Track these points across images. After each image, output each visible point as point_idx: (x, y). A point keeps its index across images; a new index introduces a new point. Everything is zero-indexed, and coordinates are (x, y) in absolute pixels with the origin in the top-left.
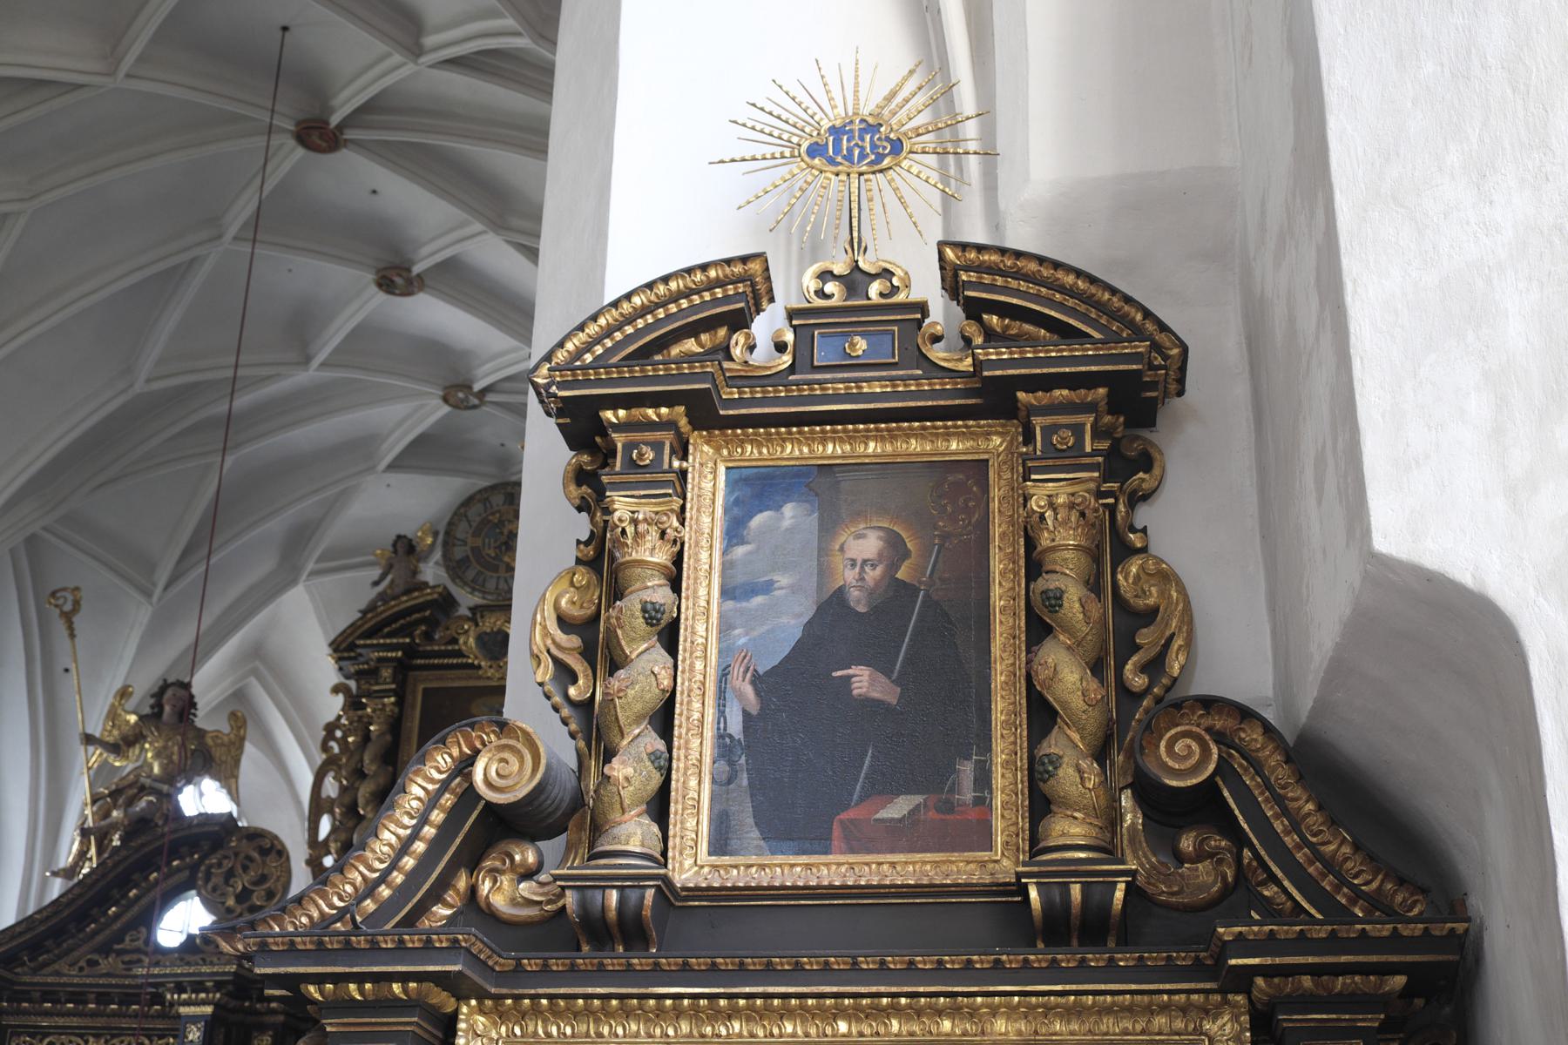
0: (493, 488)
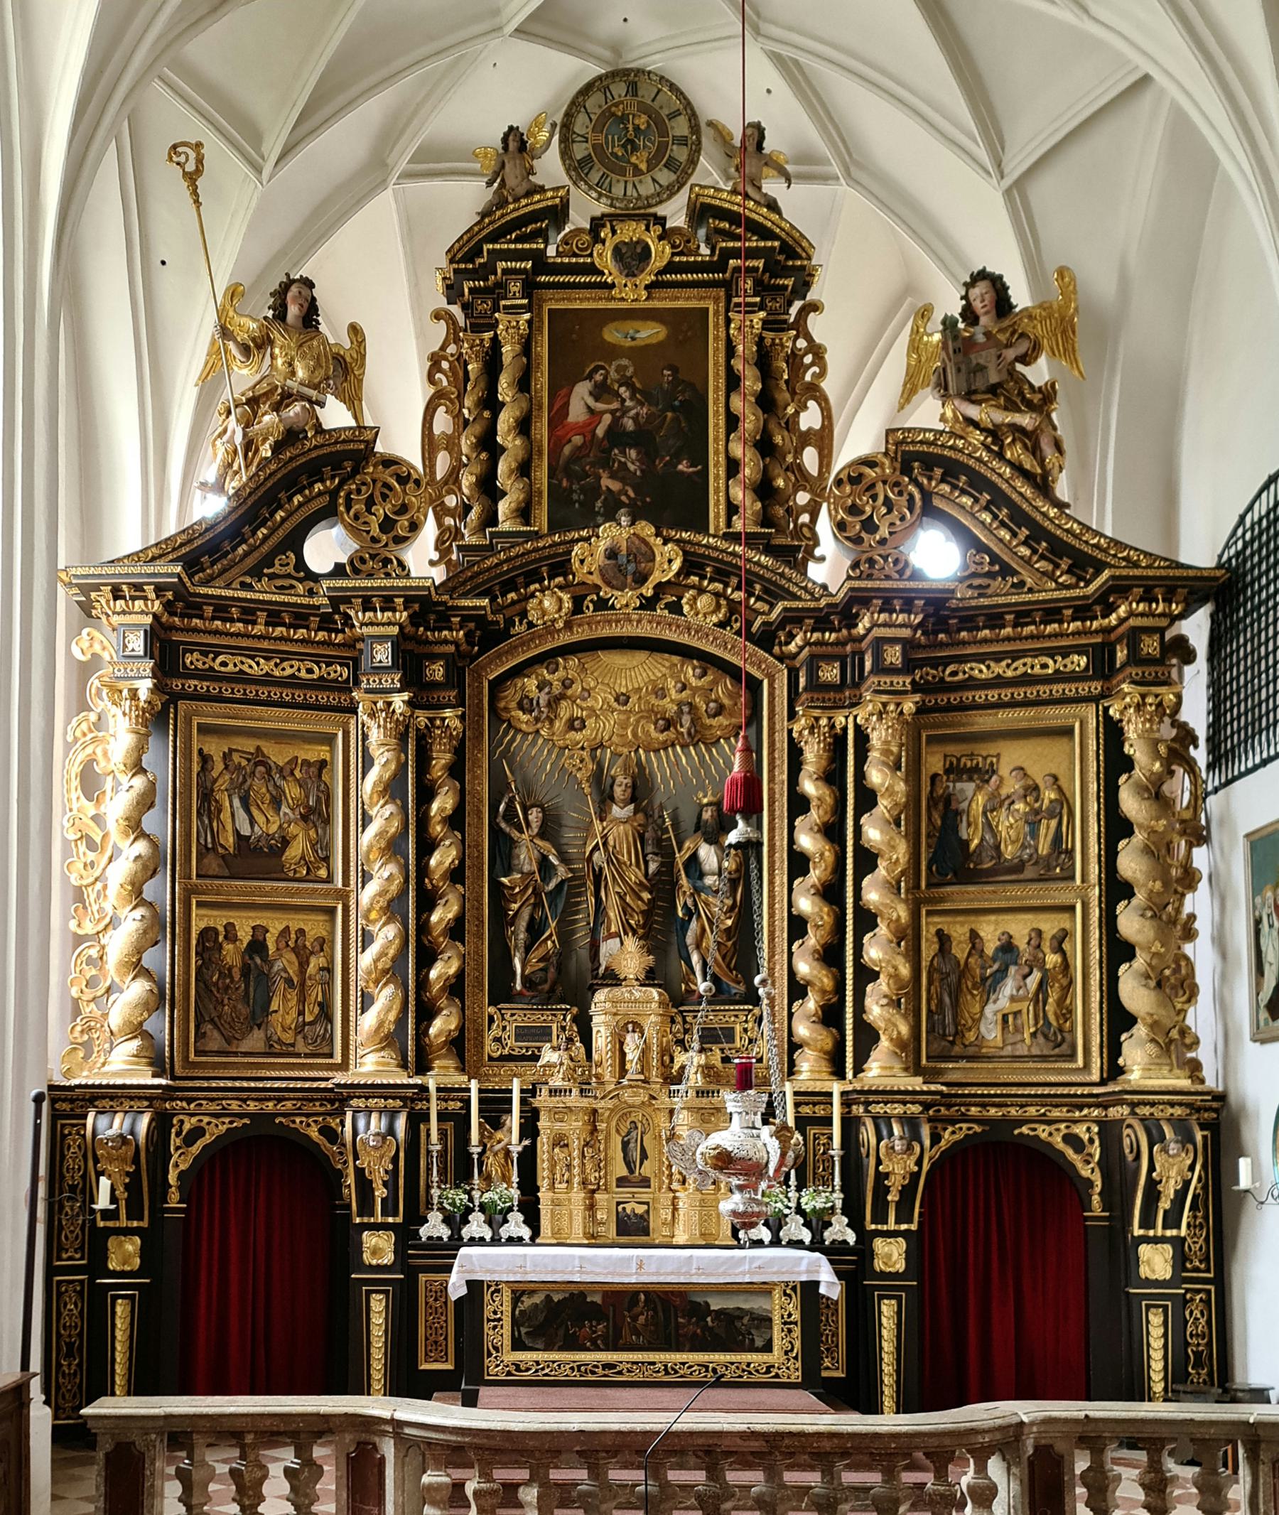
0: (614, 75)
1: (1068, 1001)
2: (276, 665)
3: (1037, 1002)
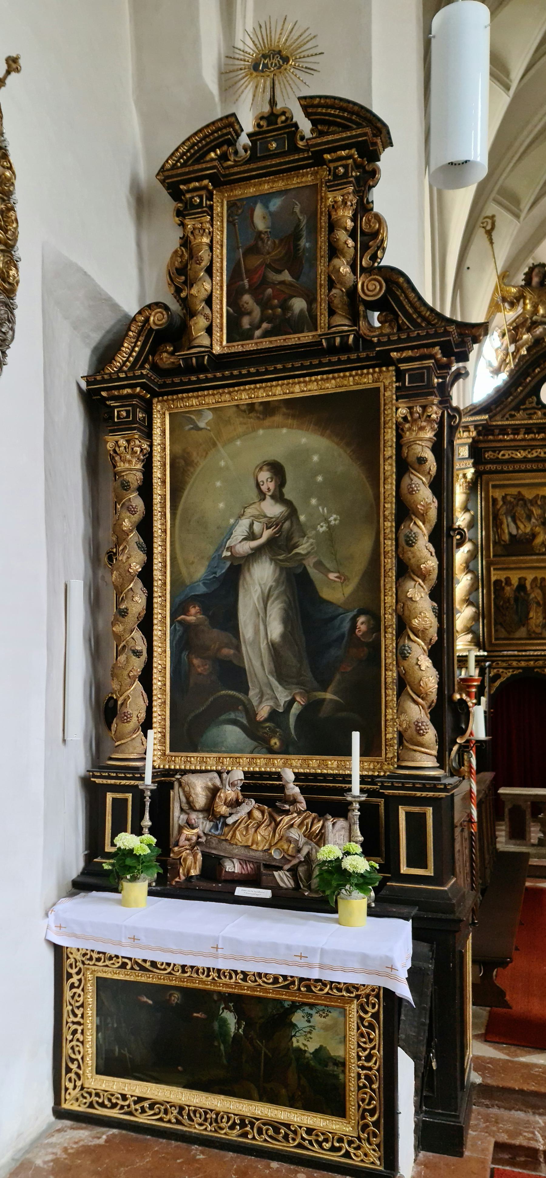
2: (529, 452)
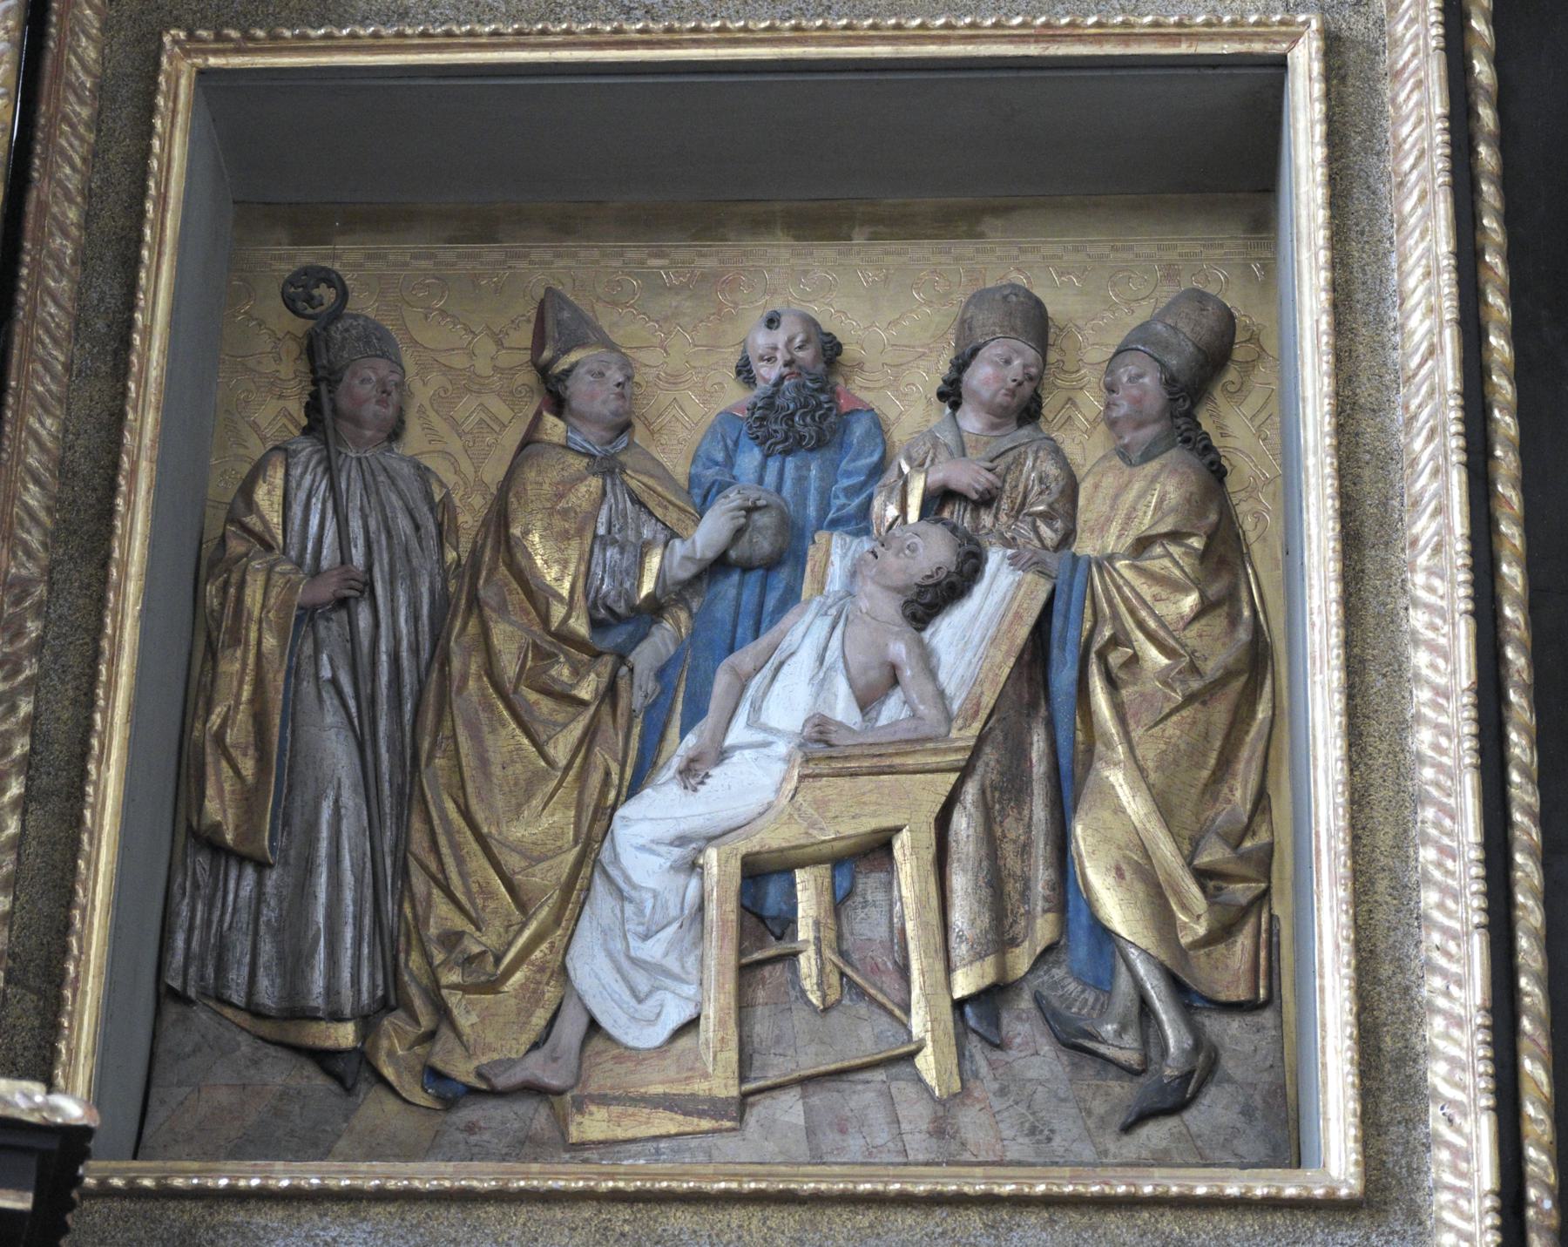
1: (1240, 793)
3: (1013, 786)
